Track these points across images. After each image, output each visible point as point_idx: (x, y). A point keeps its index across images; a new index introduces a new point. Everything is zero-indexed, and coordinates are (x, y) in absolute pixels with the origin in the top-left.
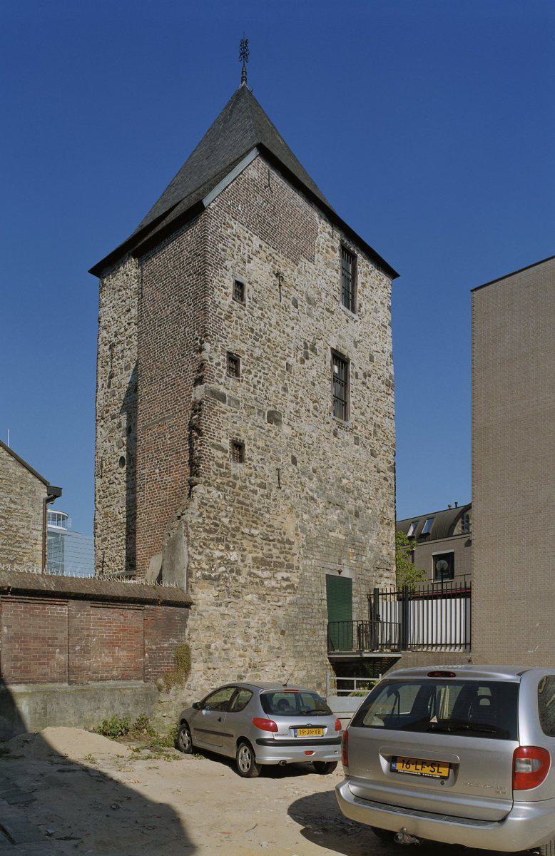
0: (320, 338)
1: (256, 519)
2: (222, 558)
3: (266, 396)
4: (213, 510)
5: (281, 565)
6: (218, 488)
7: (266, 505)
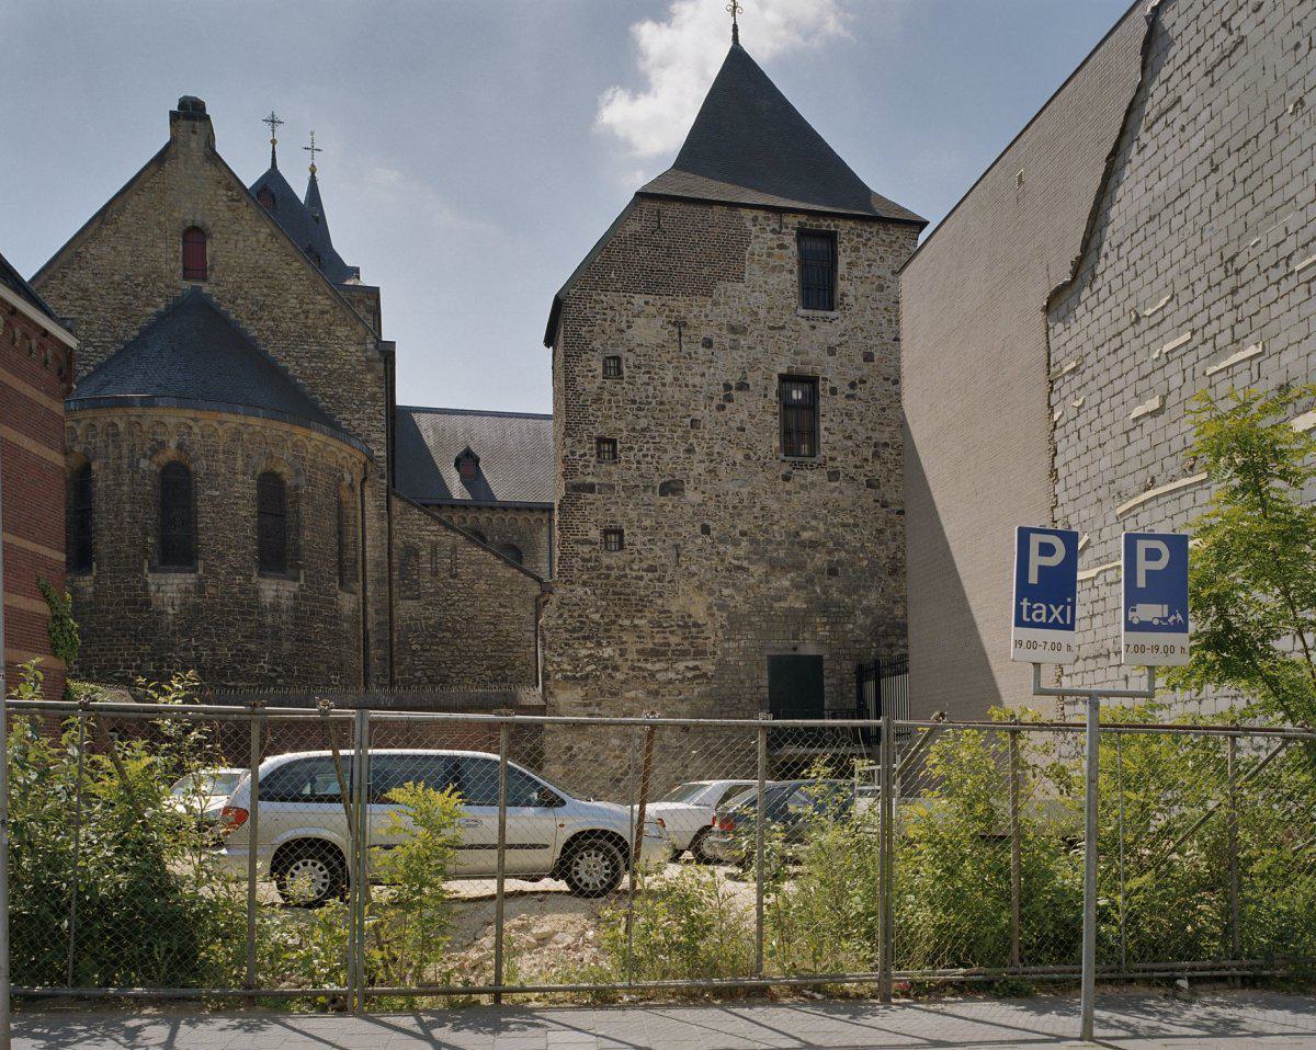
4: (577, 608)
5: (684, 653)
6: (584, 584)
7: (657, 589)
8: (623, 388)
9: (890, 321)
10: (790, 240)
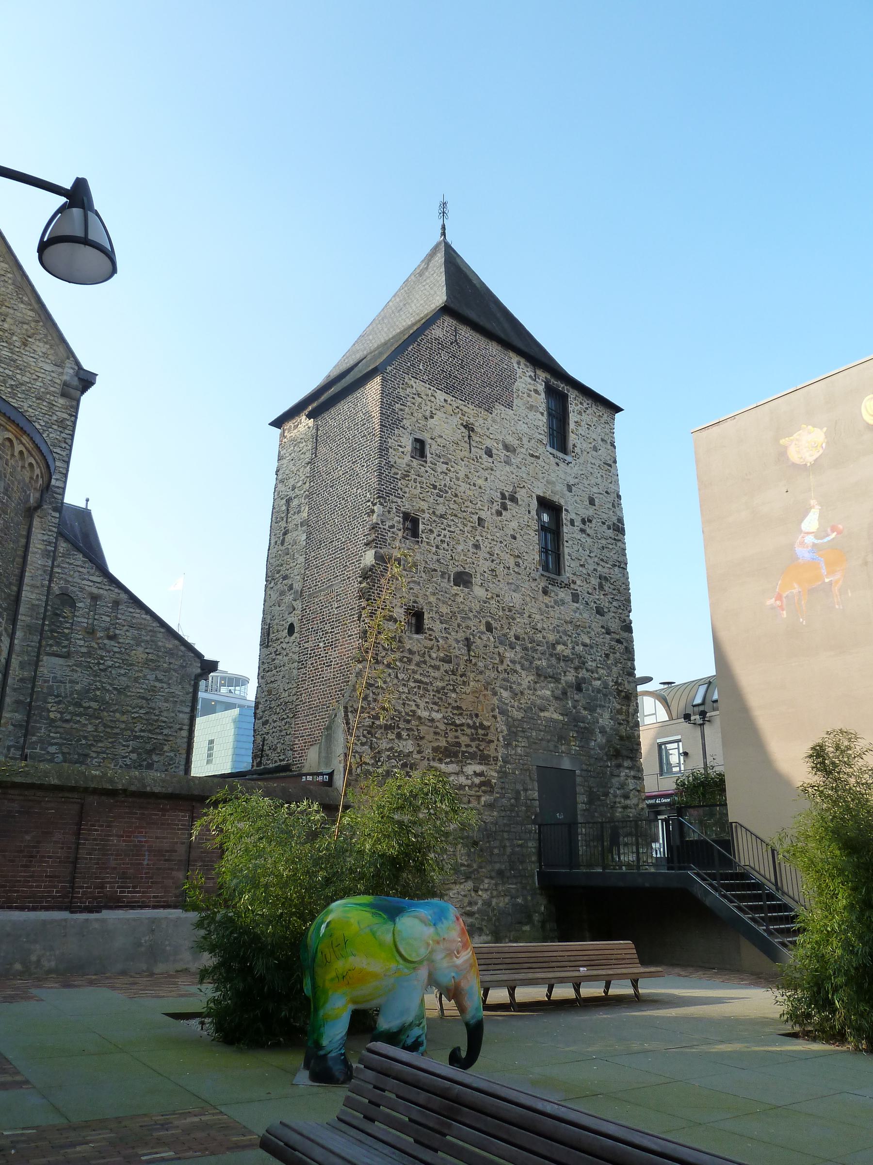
0: (522, 486)
1: (438, 701)
2: (391, 749)
3: (452, 556)
7: (452, 682)
8: (427, 472)
9: (602, 476)
10: (541, 388)
